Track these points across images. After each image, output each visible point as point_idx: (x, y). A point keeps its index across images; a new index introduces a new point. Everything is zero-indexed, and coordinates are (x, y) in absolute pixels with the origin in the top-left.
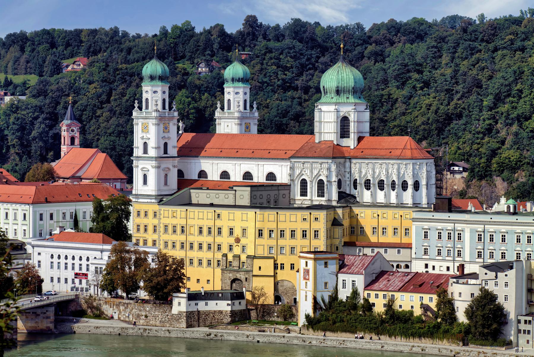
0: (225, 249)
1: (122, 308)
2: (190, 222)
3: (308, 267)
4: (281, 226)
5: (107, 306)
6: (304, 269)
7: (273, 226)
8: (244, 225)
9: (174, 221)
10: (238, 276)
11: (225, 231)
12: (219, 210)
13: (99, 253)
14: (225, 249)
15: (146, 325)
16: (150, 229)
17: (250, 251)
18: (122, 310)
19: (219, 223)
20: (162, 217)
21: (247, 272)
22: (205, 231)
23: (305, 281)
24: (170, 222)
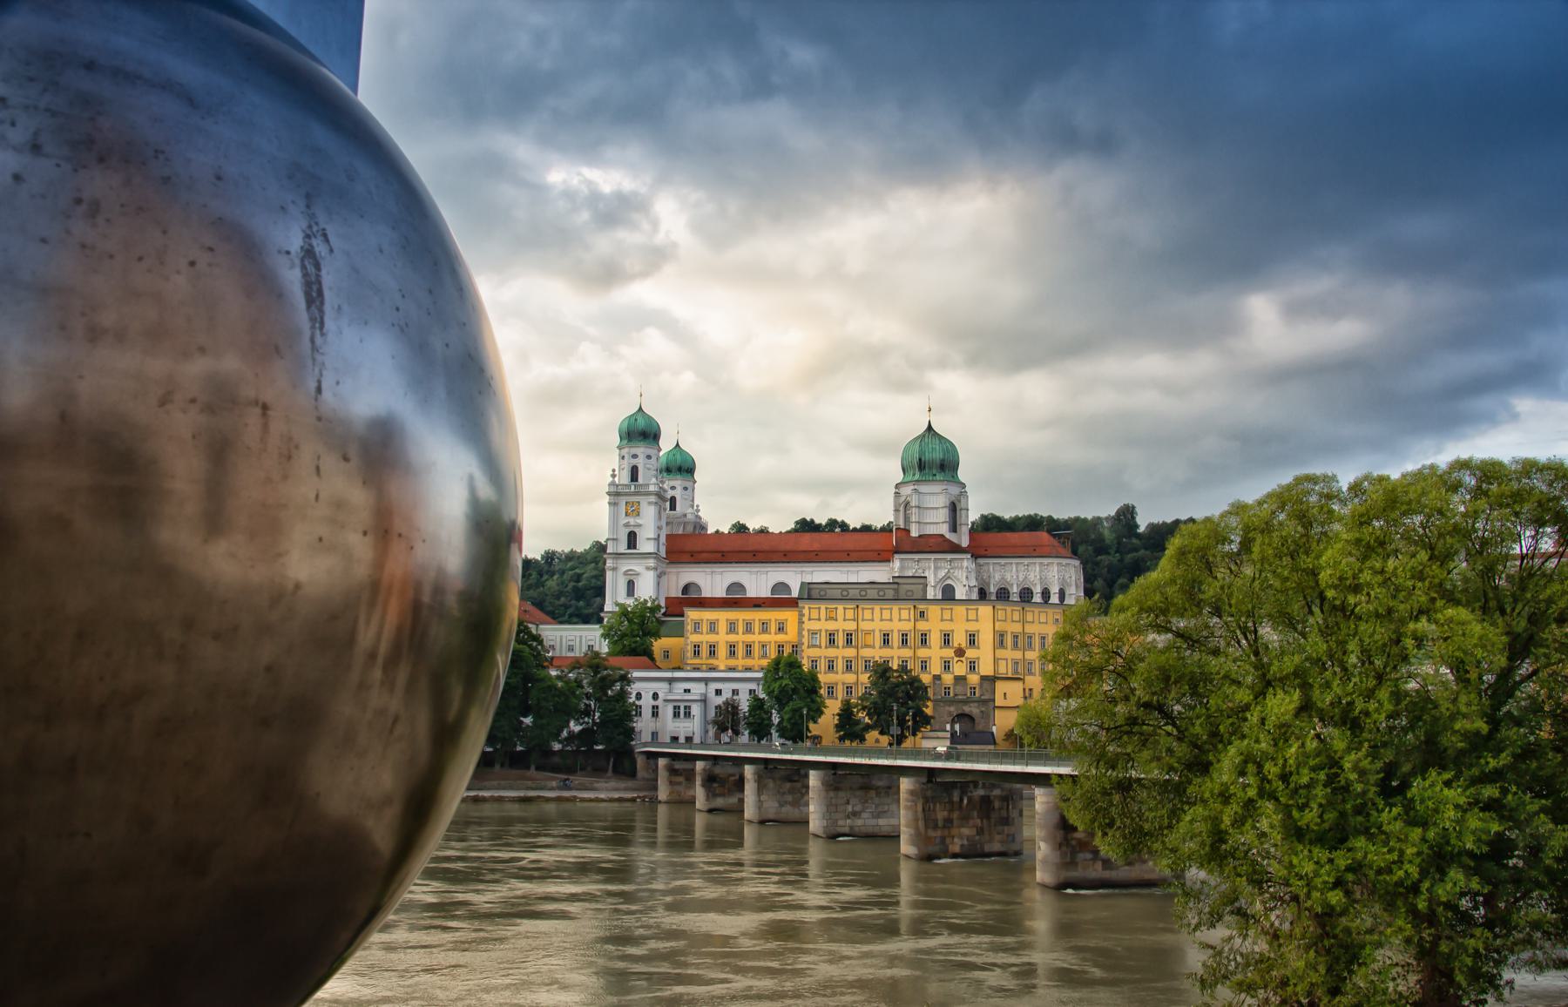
0: (936, 668)
2: (864, 626)
4: (1029, 629)
7: (1017, 628)
8: (972, 627)
9: (831, 626)
10: (967, 709)
11: (935, 639)
12: (921, 607)
13: (665, 685)
14: (936, 668)
16: (722, 651)
17: (986, 669)
19: (922, 626)
20: (805, 619)
21: (985, 702)
22: (895, 639)
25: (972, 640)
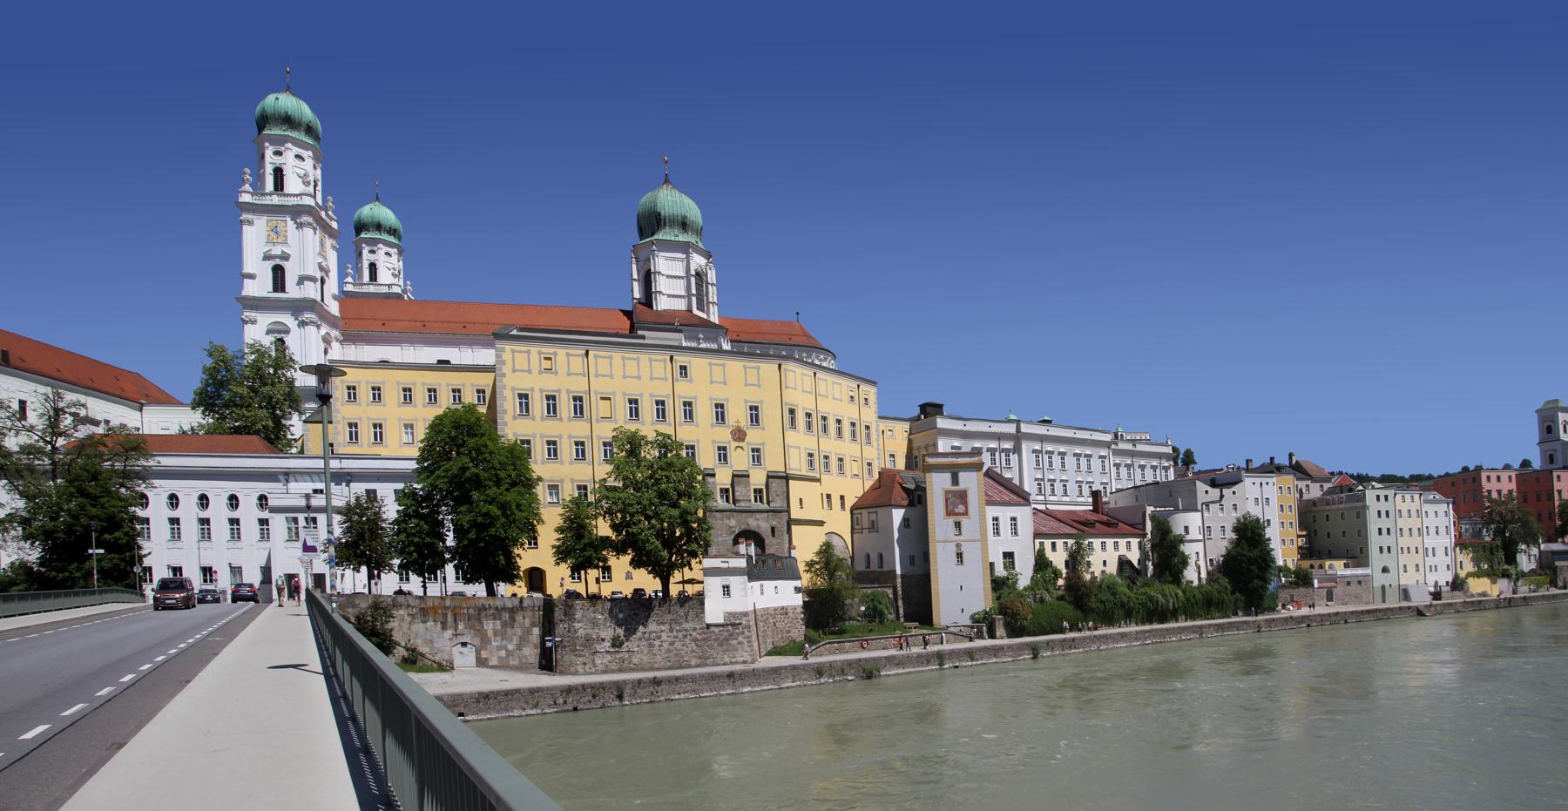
1: (490, 626)
3: (962, 486)
5: (430, 624)
6: (947, 492)
8: (754, 397)
11: (704, 412)
15: (620, 671)
18: (490, 633)
23: (951, 520)
24: (539, 385)
25: (755, 414)
